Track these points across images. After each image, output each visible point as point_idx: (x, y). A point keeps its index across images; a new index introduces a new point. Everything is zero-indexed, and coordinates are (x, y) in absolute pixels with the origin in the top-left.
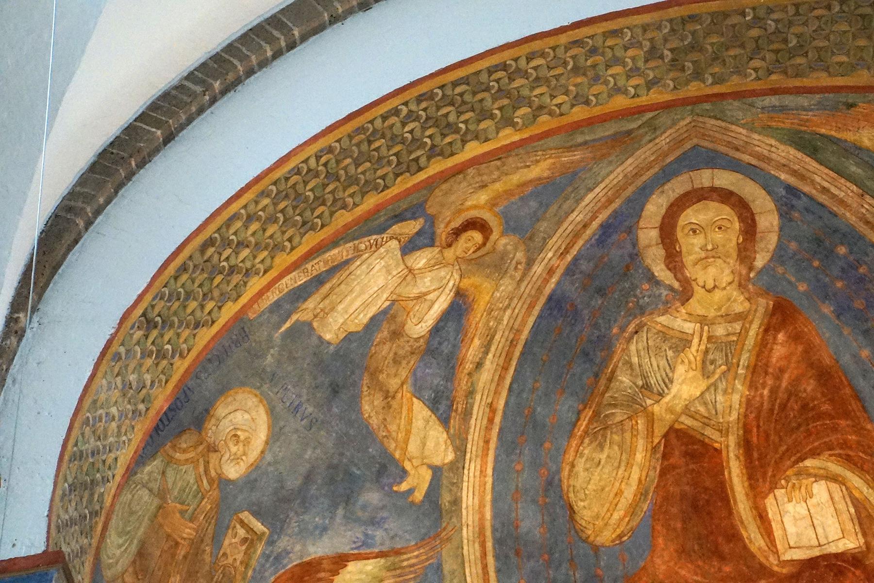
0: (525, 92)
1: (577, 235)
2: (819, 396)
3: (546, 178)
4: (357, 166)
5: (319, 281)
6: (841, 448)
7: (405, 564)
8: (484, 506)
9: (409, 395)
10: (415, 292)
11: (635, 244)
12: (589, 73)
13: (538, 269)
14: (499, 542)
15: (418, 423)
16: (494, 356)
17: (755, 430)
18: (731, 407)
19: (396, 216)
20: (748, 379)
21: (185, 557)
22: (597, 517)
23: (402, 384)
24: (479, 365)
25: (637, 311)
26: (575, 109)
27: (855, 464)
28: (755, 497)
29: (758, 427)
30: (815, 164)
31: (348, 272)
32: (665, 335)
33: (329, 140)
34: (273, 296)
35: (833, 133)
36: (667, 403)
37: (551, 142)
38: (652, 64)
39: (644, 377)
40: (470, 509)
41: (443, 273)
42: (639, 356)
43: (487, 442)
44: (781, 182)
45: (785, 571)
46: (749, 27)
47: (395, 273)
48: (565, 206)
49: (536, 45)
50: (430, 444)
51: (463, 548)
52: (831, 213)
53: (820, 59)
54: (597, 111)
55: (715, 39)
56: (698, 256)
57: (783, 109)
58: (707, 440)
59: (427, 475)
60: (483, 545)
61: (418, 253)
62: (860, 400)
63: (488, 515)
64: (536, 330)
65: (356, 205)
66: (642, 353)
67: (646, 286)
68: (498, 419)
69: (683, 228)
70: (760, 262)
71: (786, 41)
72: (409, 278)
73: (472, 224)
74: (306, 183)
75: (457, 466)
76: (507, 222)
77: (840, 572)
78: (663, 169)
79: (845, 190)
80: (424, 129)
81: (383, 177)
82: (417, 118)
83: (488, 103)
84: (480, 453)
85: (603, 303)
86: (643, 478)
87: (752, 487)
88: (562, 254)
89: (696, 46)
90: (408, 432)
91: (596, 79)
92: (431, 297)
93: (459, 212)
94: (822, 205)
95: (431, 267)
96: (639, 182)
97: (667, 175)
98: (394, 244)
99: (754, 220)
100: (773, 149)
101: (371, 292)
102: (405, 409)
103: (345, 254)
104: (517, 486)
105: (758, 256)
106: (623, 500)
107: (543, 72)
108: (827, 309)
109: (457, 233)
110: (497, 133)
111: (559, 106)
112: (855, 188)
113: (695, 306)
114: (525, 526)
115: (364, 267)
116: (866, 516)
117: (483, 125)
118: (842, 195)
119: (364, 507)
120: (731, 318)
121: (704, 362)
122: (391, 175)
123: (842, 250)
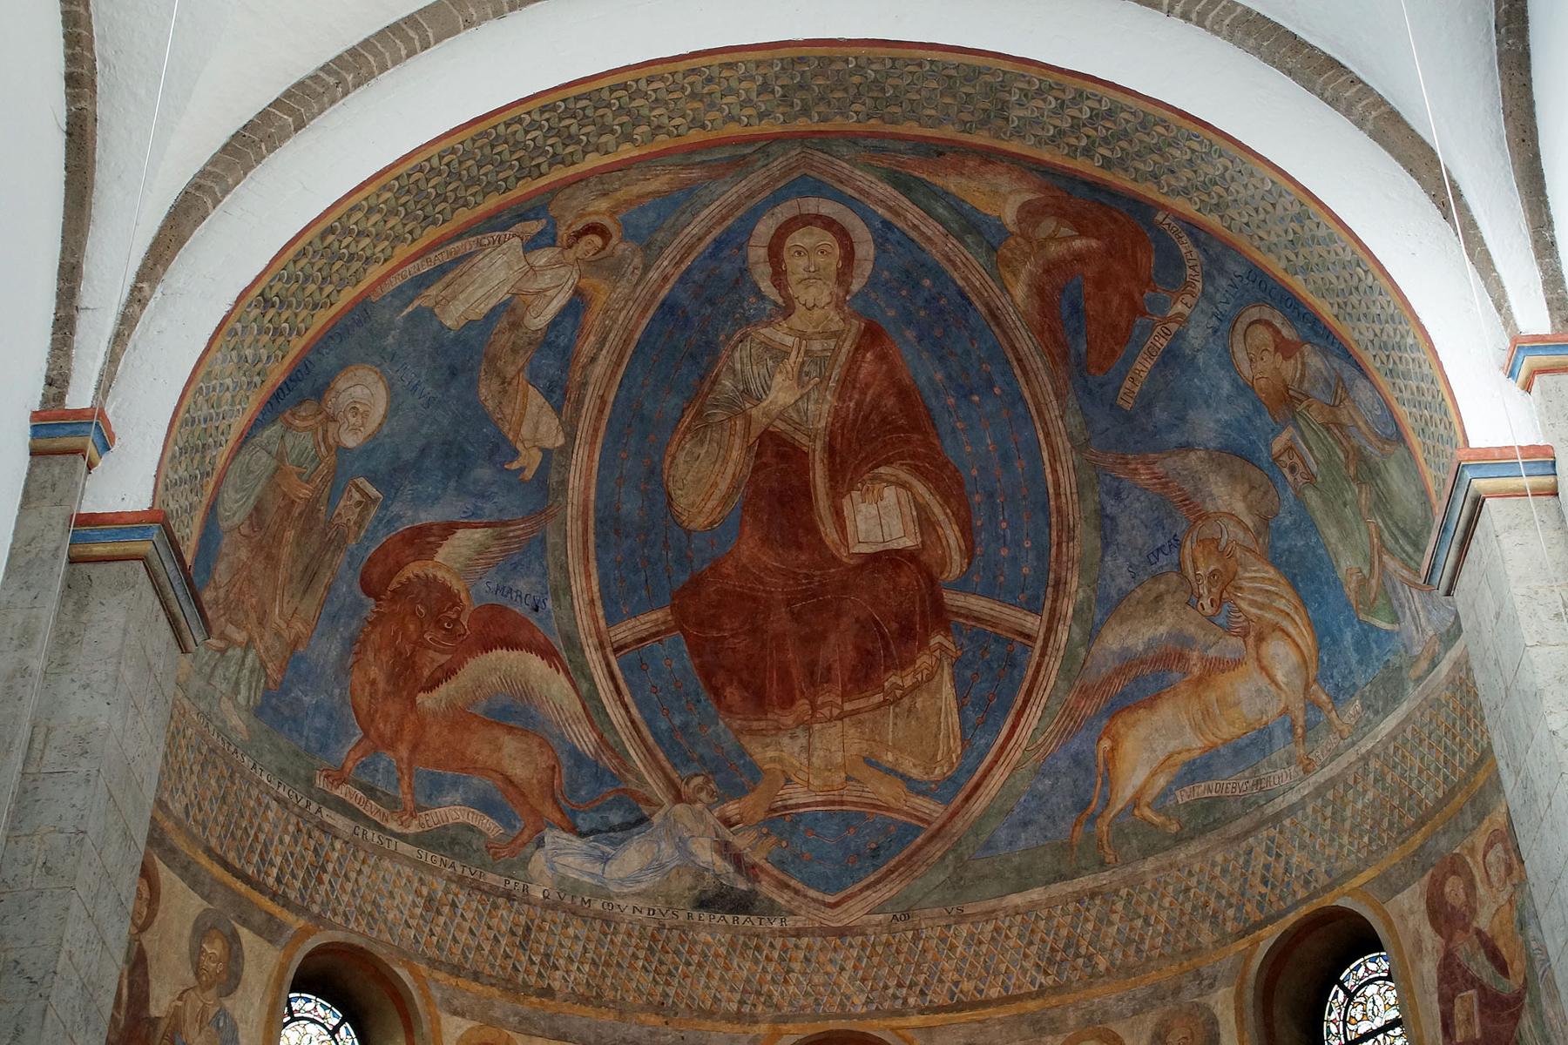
0: (645, 112)
1: (691, 247)
4: (480, 167)
5: (442, 270)
10: (536, 286)
11: (745, 260)
13: (654, 275)
14: (600, 521)
15: (532, 409)
19: (519, 216)
21: (301, 514)
22: (693, 505)
23: (518, 373)
24: (593, 360)
25: (743, 322)
29: (843, 435)
32: (767, 346)
33: (453, 141)
34: (395, 282)
35: (924, 176)
37: (669, 160)
38: (764, 97)
39: (746, 383)
41: (562, 271)
42: (742, 363)
43: (596, 430)
45: (852, 562)
46: (852, 74)
48: (682, 219)
49: (658, 69)
50: (543, 429)
54: (712, 135)
55: (821, 81)
56: (801, 276)
57: (884, 150)
59: (537, 457)
63: (592, 497)
64: (648, 332)
68: (607, 411)
69: (789, 248)
70: (856, 286)
71: (883, 90)
74: (428, 181)
75: (566, 451)
77: (898, 566)
79: (932, 229)
80: (546, 137)
81: (505, 180)
82: (540, 127)
87: (832, 487)
90: (523, 415)
91: (712, 105)
93: (581, 216)
94: (913, 241)
97: (776, 200)
98: (517, 241)
99: (852, 248)
101: (493, 284)
107: (663, 95)
108: (910, 334)
109: (579, 235)
112: (941, 228)
113: (794, 320)
114: (626, 508)
117: (604, 139)
118: (929, 233)
119: (475, 482)
120: (827, 335)
121: (800, 372)
122: (512, 179)
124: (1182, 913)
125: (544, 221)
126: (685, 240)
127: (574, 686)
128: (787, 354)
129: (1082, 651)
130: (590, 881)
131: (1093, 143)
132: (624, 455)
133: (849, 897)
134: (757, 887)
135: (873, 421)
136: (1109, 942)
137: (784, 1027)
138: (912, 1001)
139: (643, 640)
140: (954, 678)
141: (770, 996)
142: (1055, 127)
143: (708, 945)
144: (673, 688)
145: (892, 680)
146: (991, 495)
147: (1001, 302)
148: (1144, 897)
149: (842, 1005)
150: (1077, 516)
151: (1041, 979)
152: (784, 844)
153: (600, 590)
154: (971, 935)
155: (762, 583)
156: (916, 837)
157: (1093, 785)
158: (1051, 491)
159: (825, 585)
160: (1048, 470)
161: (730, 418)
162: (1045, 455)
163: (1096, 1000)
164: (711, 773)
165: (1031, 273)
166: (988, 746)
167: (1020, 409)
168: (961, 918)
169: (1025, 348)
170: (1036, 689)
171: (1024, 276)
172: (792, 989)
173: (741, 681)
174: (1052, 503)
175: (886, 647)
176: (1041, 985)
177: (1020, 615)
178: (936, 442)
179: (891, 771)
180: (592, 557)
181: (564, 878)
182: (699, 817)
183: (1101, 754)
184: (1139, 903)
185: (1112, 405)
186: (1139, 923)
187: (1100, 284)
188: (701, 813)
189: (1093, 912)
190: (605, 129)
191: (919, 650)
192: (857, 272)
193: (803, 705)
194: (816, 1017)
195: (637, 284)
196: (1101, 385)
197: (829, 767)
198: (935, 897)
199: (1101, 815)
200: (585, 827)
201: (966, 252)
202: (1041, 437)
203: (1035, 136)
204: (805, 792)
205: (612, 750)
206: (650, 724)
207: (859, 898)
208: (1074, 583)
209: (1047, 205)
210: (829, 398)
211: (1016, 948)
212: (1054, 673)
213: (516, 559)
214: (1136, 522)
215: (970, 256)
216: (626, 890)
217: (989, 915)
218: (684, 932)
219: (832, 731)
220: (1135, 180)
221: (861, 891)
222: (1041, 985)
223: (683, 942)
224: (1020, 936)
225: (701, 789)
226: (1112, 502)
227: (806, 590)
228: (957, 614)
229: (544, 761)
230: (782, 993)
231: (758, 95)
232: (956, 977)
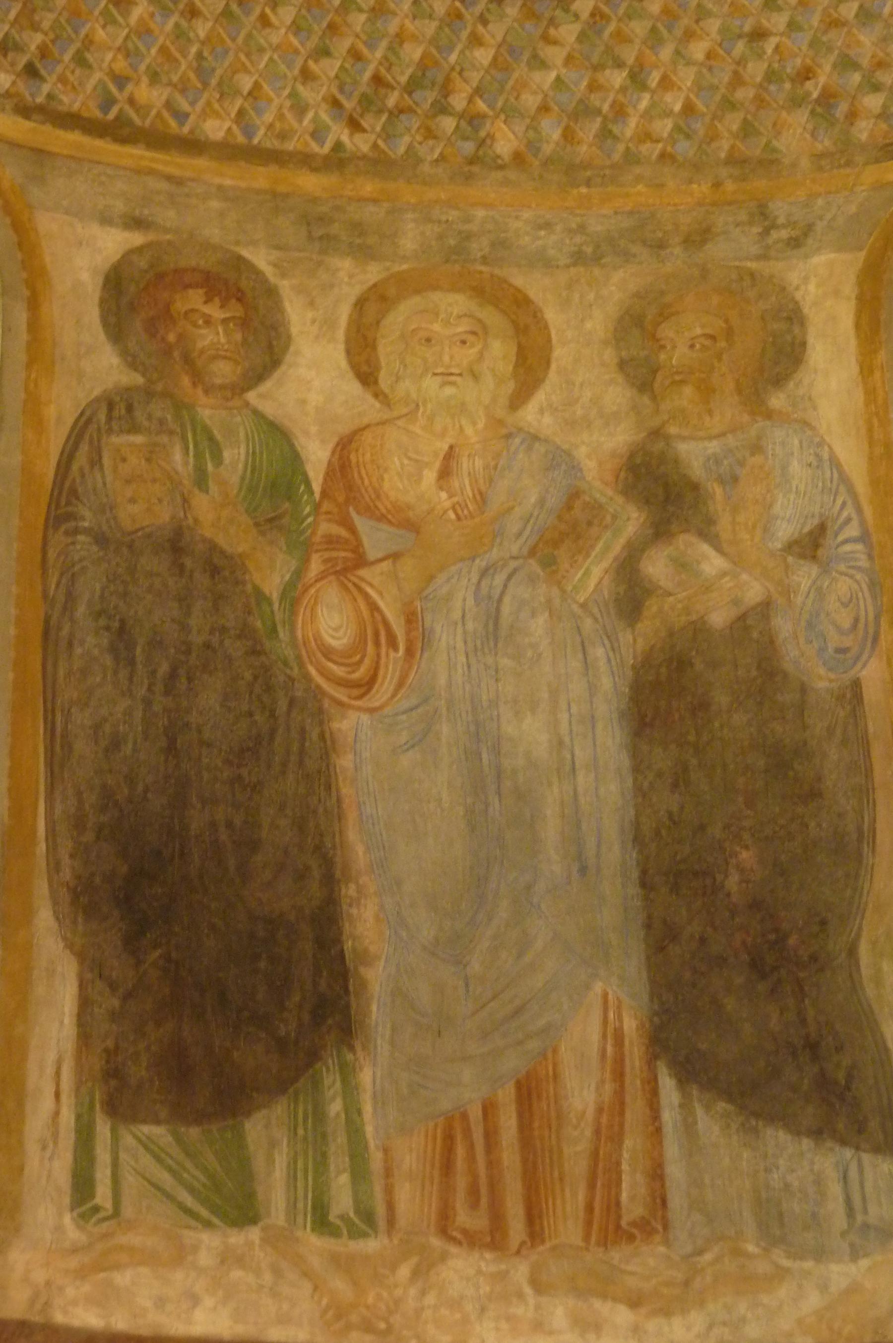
124: (737, 81)
136: (530, 101)
148: (639, 28)
151: (339, 132)
176: (338, 146)
184: (620, 37)
186: (617, 78)
222: (338, 146)
224: (296, 28)
232: (121, 65)
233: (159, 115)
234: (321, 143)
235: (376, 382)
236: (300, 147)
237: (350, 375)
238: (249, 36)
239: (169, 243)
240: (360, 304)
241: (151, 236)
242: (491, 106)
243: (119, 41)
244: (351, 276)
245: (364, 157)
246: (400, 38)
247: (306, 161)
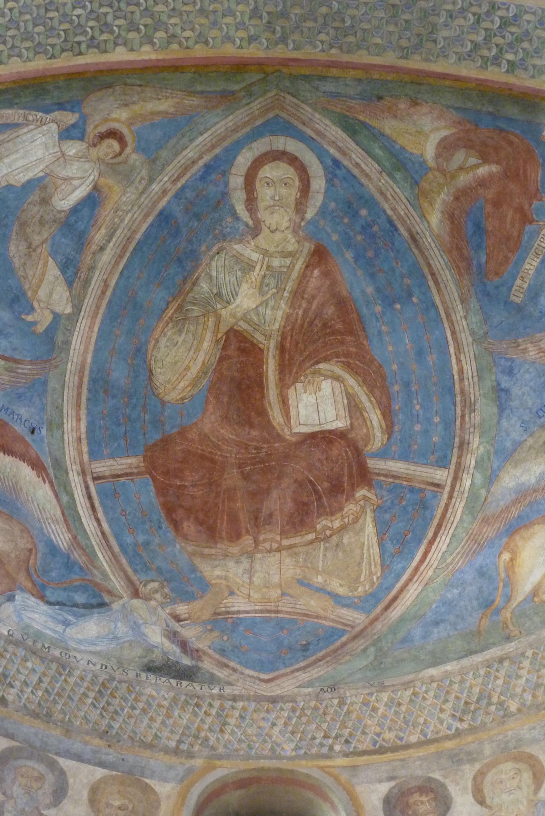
0: (164, 18)
1: (186, 169)
2: (336, 317)
3: (171, 114)
4: (35, 25)
6: (346, 358)
7: (20, 371)
8: (87, 353)
9: (46, 253)
10: (64, 173)
11: (226, 185)
12: (210, 17)
13: (156, 187)
14: (93, 381)
16: (114, 245)
17: (289, 338)
18: (275, 319)
20: (290, 301)
22: (168, 382)
23: (43, 243)
24: (102, 249)
26: (198, 46)
27: (352, 369)
28: (282, 387)
29: (292, 336)
30: (353, 144)
31: (15, 135)
32: (238, 258)
35: (367, 120)
36: (232, 310)
38: (254, 22)
39: (219, 288)
40: (77, 351)
41: (87, 166)
43: (98, 307)
44: (330, 155)
45: (294, 439)
47: (51, 151)
50: (55, 296)
51: (65, 376)
52: (359, 183)
53: (364, 40)
55: (298, 11)
58: (255, 341)
59: (48, 318)
60: (81, 379)
61: (71, 143)
62: (362, 323)
64: (147, 235)
65: (28, 60)
66: (220, 269)
67: (230, 220)
68: (109, 293)
69: (261, 179)
70: (309, 215)
71: (343, 21)
72: (62, 160)
73: (112, 134)
75: (73, 318)
76: (139, 142)
77: (331, 442)
78: (252, 130)
80: (88, 19)
81: (53, 46)
83: (137, 16)
84: (91, 315)
85: (197, 226)
86: (206, 361)
87: (281, 380)
88: (174, 180)
89: (284, 15)
90: (41, 281)
91: (215, 23)
92: (76, 183)
93: (106, 120)
94: (355, 177)
95: (78, 157)
96: (235, 137)
98: (54, 126)
99: (308, 181)
100: (327, 128)
101: (32, 159)
102: (41, 262)
103: (16, 117)
104: (114, 346)
105: (308, 210)
106: (189, 374)
108: (349, 255)
109: (103, 137)
110: (141, 46)
111: (187, 39)
112: (376, 166)
113: (261, 240)
114: (115, 375)
115: (29, 135)
116: (354, 406)
118: (368, 171)
120: (285, 254)
121: (261, 284)
122: (58, 48)
123: (364, 212)
125: (77, 115)
126: (183, 161)
127: (57, 496)
128: (253, 268)
129: (483, 492)
130: (53, 634)
131: (501, 51)
132: (118, 332)
133: (283, 675)
134: (200, 664)
135: (316, 326)
136: (519, 690)
137: (218, 763)
138: (337, 748)
139: (118, 476)
140: (376, 521)
141: (206, 739)
142: (472, 42)
143: (153, 697)
144: (139, 514)
145: (323, 523)
146: (407, 385)
147: (420, 227)
149: (272, 750)
150: (477, 394)
152: (225, 638)
153: (87, 432)
154: (392, 700)
155: (220, 450)
156: (341, 636)
157: (497, 589)
158: (456, 377)
159: (271, 454)
160: (454, 361)
161: (204, 315)
162: (452, 350)
163: (510, 733)
164: (166, 580)
165: (444, 201)
166: (404, 569)
167: (432, 313)
168: (382, 688)
169: (438, 264)
170: (445, 524)
171: (438, 205)
172: (226, 737)
173: (197, 519)
174: (457, 386)
175: (319, 499)
176: (457, 729)
177: (430, 471)
178: (365, 342)
179: (320, 590)
180: (83, 405)
181: (28, 626)
182: (153, 611)
183: (502, 564)
185: (506, 303)
187: (497, 204)
188: (155, 609)
189: (503, 672)
190: (133, 27)
191: (347, 500)
192: (311, 202)
193: (247, 540)
194: (248, 757)
195: (143, 192)
196: (497, 287)
197: (267, 585)
198: (358, 676)
199: (504, 608)
200: (52, 600)
201: (395, 187)
202: (449, 334)
203: (456, 53)
204: (245, 603)
205: (84, 550)
206: (117, 537)
207: (290, 677)
208: (475, 442)
209: (459, 139)
210: (283, 305)
211: (433, 705)
212: (460, 510)
213: (21, 391)
214: (526, 389)
215: (398, 190)
216: (82, 648)
217: (406, 685)
218: (132, 686)
219: (272, 559)
220: (533, 77)
221: (293, 672)
222: (457, 729)
223: (130, 692)
224: (435, 697)
225: (156, 591)
226: (506, 378)
227: (254, 458)
228: (378, 474)
229: (23, 543)
230: (218, 739)
231: (250, 18)
232: (378, 730)
233: (394, 741)
234: (451, 730)
235: (485, 802)
236: (444, 734)
237: (476, 803)
238: (420, 705)
239: (404, 781)
240: (475, 778)
241: (398, 781)
242: (506, 697)
243: (376, 722)
244: (470, 770)
245: (466, 729)
246: (471, 687)
247: (447, 738)
